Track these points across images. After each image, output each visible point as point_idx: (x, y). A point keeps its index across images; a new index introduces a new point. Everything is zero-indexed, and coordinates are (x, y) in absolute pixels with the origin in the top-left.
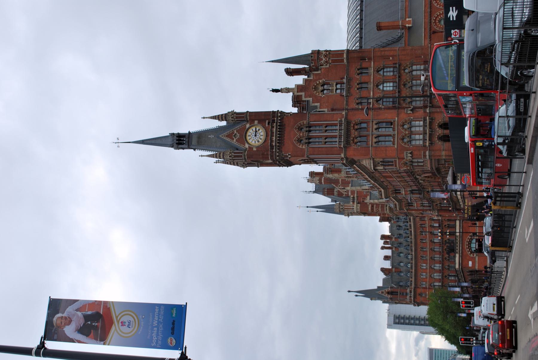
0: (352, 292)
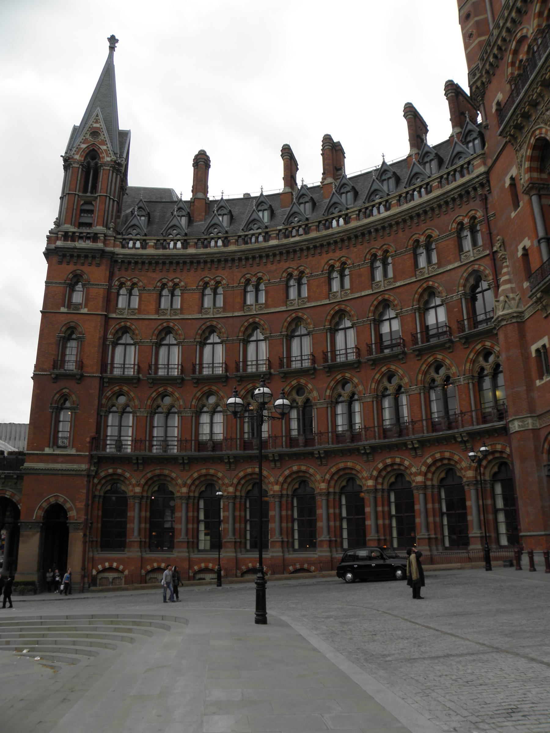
0: (112, 48)
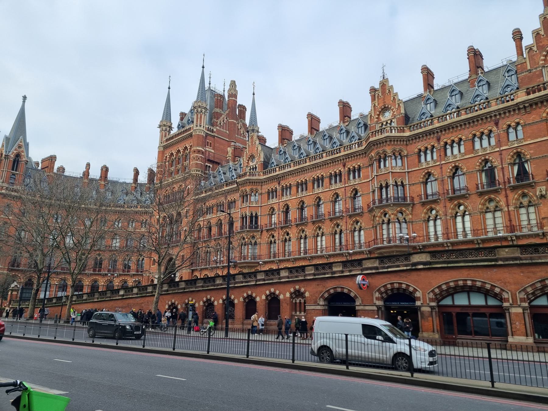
0: (24, 102)
